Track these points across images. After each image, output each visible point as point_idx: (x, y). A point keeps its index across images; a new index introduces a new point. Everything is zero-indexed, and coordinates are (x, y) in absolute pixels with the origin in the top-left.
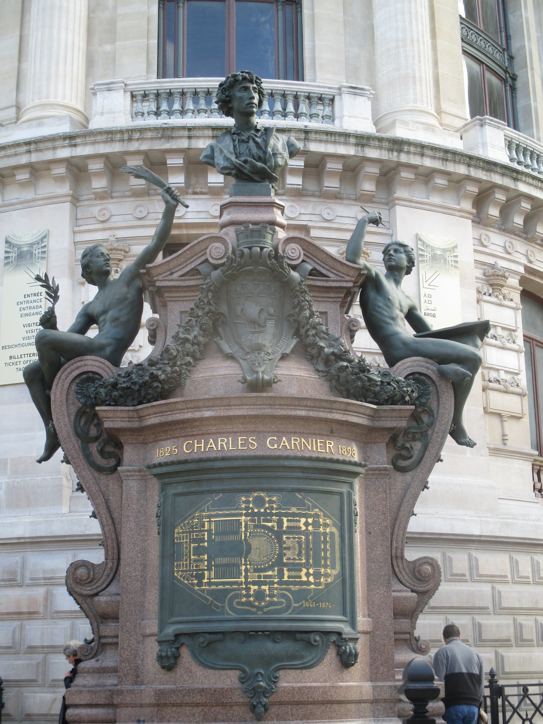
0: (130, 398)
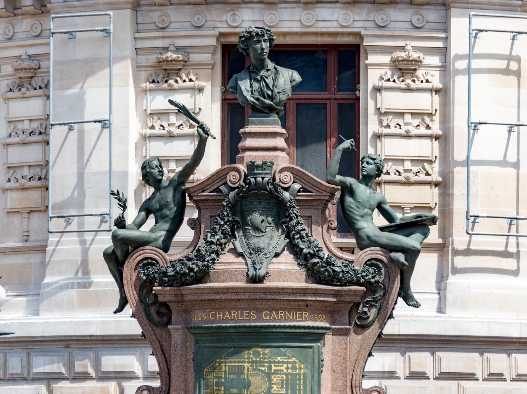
0: (175, 282)
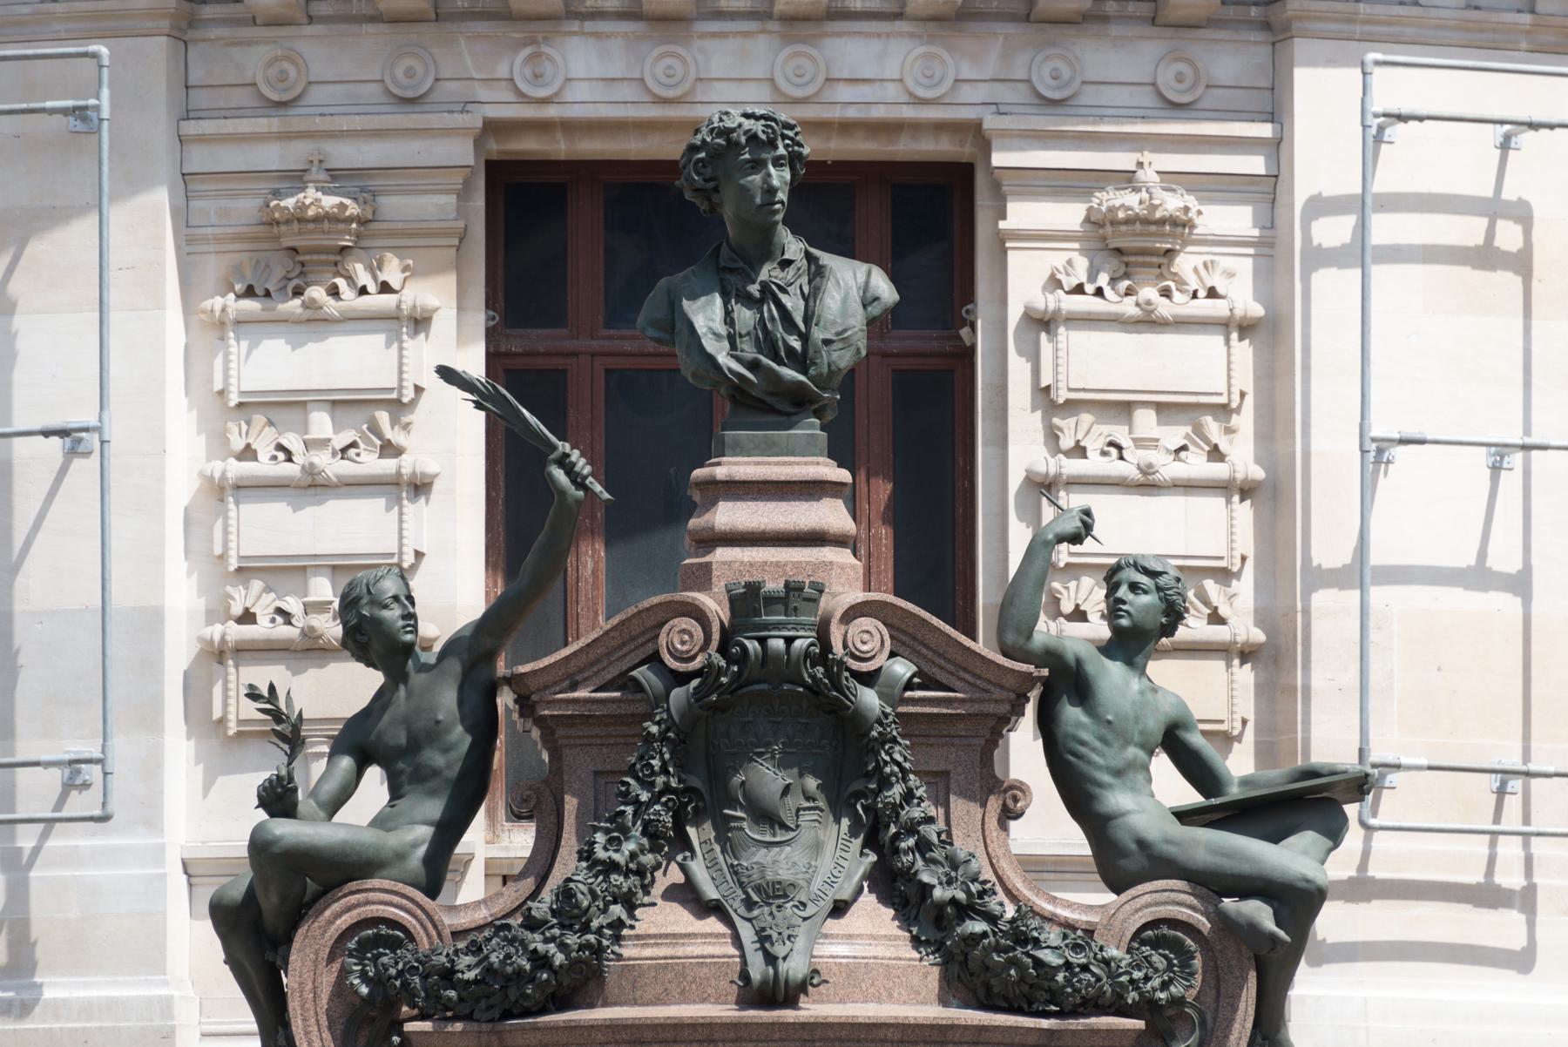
0: (483, 1004)
